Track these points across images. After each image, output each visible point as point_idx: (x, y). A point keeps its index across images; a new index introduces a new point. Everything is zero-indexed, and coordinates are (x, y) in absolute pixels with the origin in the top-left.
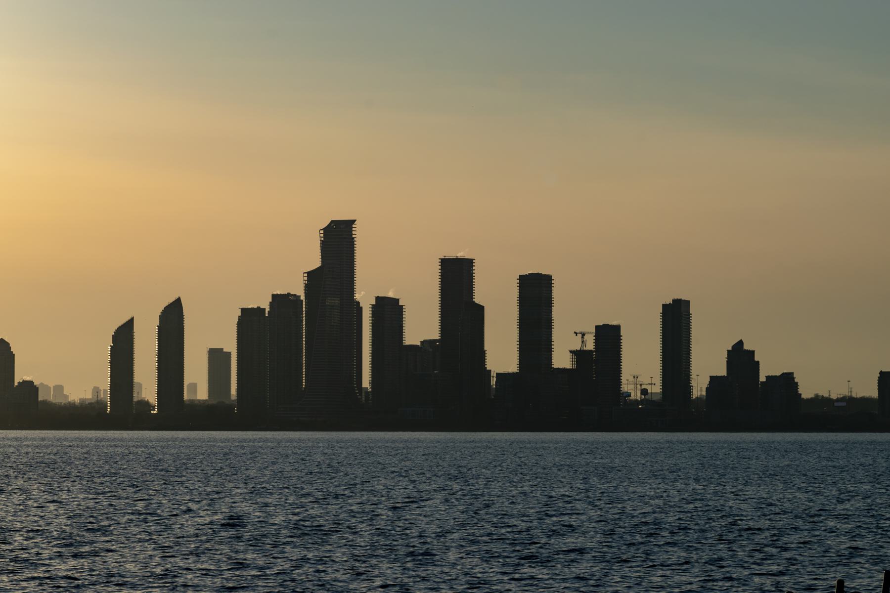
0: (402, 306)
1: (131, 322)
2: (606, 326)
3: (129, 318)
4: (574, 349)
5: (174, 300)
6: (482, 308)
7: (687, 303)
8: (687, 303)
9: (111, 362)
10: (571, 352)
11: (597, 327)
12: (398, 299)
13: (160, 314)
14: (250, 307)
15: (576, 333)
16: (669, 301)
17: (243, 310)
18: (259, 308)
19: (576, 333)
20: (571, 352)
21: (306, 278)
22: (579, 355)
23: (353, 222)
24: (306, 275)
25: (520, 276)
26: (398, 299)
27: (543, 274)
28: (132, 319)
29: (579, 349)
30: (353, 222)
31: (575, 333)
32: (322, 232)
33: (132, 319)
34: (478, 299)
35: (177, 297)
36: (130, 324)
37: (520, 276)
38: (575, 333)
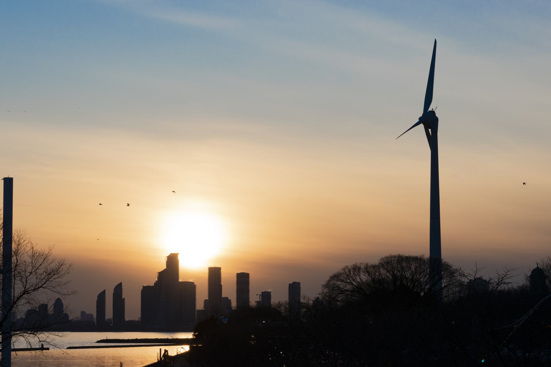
0: (195, 285)
1: (104, 292)
2: (265, 292)
3: (104, 290)
4: (257, 300)
5: (119, 283)
6: (221, 286)
7: (299, 283)
8: (299, 283)
9: (97, 307)
10: (256, 302)
11: (262, 293)
12: (194, 283)
13: (114, 288)
14: (145, 285)
15: (257, 295)
16: (291, 282)
17: (144, 287)
18: (149, 286)
19: (257, 295)
20: (256, 302)
21: (158, 275)
22: (258, 302)
23: (178, 254)
24: (158, 273)
25: (237, 273)
26: (194, 283)
27: (246, 272)
28: (105, 290)
29: (259, 300)
30: (178, 254)
31: (257, 295)
32: (167, 257)
33: (105, 290)
34: (222, 284)
35: (121, 282)
36: (104, 292)
37: (237, 273)
38: (257, 295)
